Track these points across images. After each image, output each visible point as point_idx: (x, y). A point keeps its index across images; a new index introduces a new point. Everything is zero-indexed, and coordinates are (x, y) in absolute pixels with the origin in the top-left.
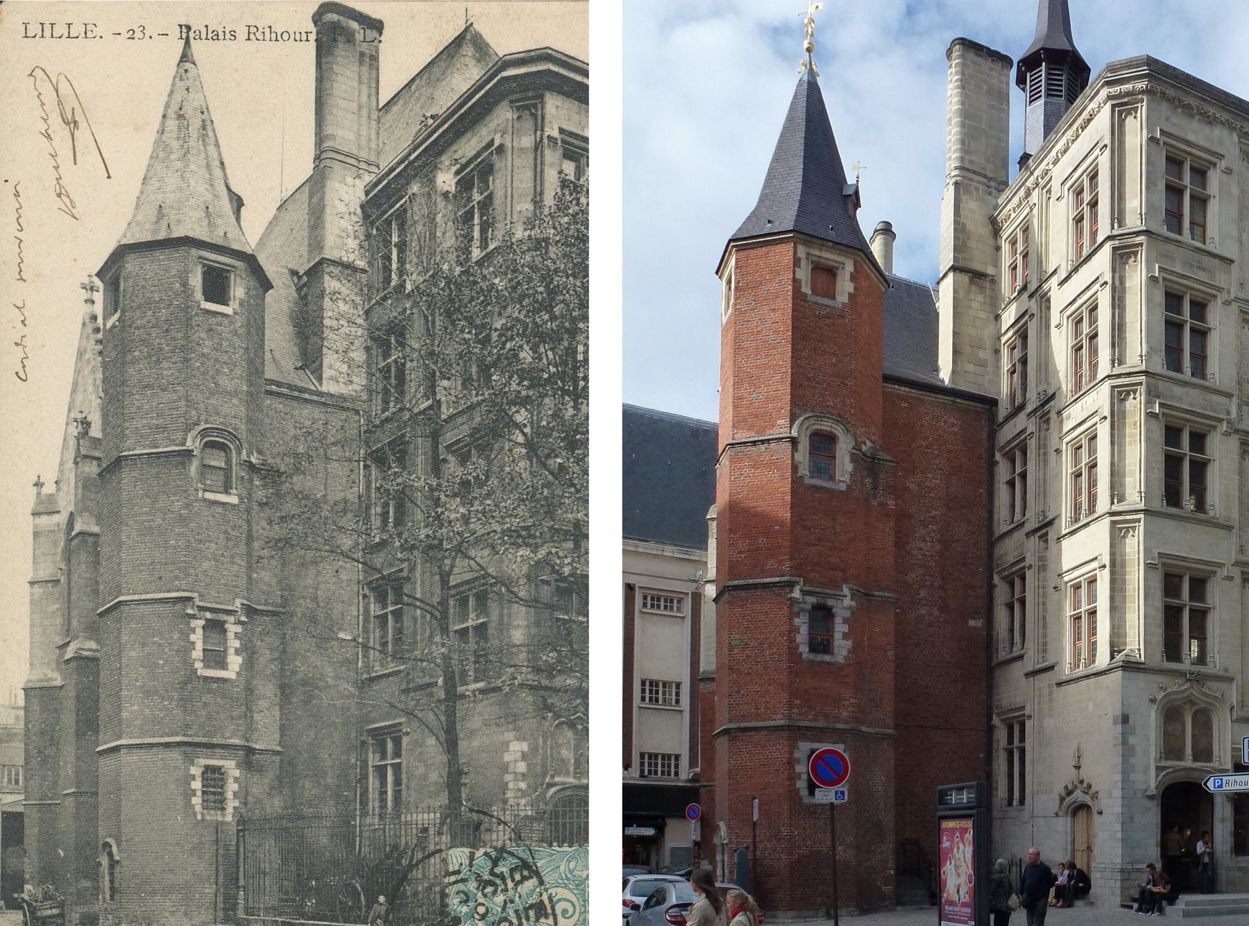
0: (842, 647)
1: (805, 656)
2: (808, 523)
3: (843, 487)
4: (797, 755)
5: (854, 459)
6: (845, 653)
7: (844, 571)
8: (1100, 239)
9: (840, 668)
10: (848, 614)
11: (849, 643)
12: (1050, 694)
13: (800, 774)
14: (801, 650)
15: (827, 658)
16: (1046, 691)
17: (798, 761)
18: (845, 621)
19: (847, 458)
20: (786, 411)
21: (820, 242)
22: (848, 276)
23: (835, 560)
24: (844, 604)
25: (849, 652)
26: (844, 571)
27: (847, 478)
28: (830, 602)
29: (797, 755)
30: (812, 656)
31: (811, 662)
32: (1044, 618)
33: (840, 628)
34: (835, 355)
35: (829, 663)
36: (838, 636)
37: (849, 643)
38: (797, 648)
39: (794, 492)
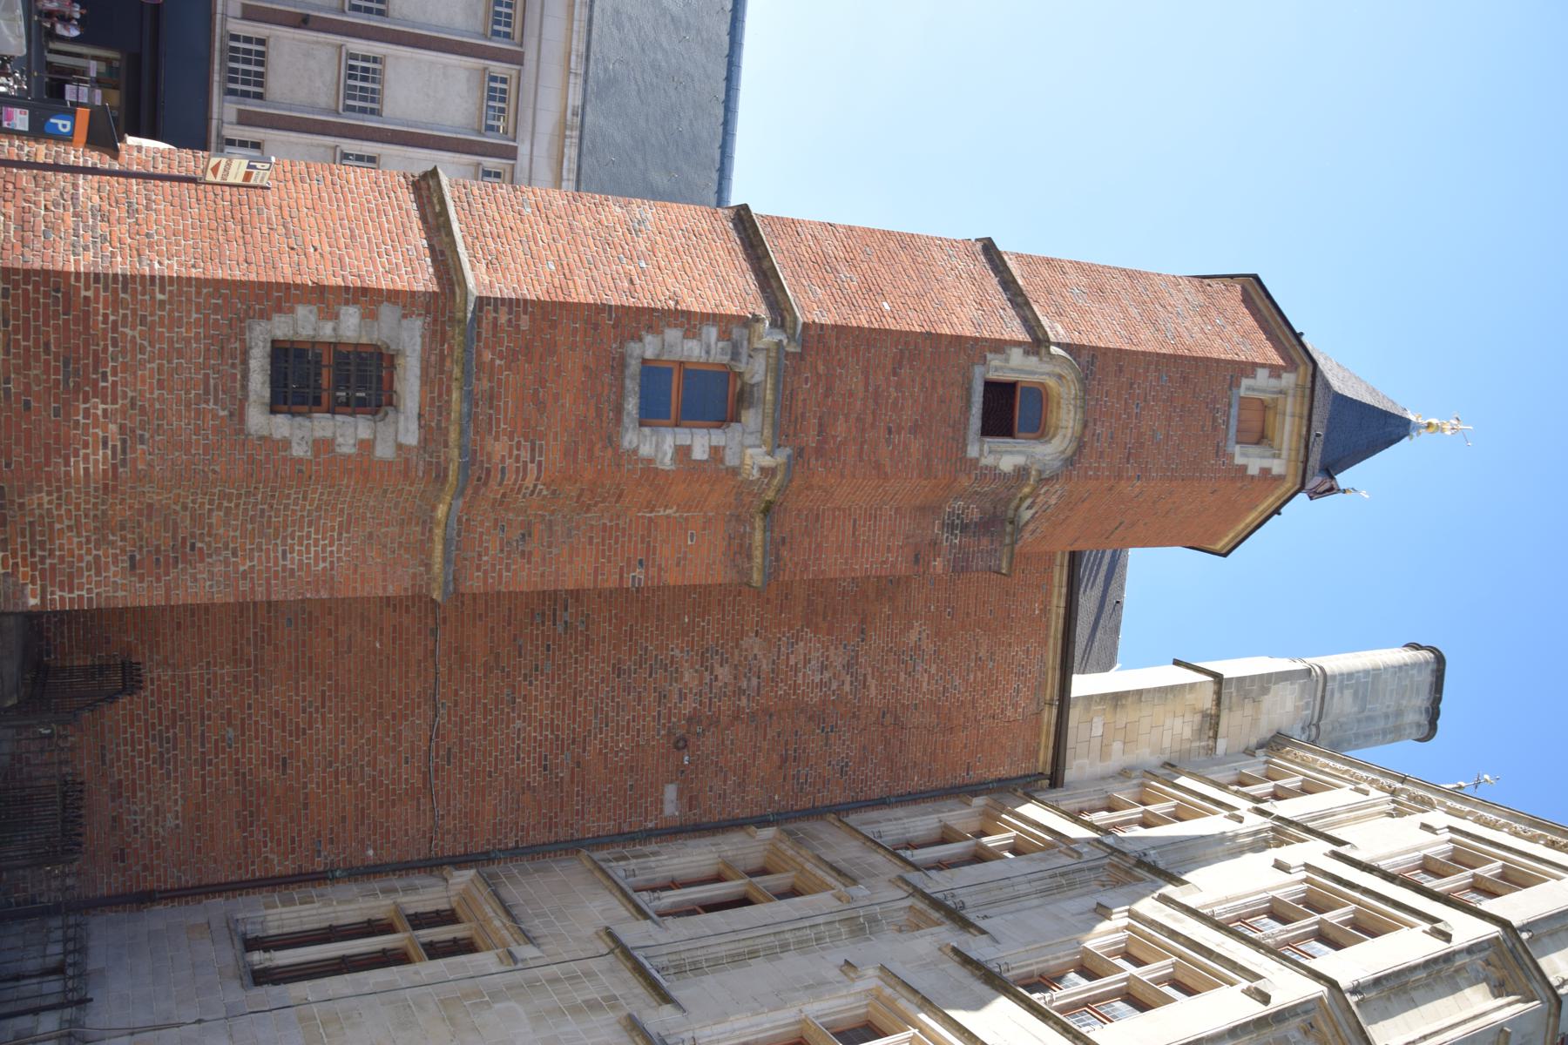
0: (658, 446)
1: (634, 349)
2: (905, 371)
3: (973, 451)
4: (388, 312)
5: (1021, 473)
6: (646, 450)
7: (819, 451)
8: (1488, 905)
9: (611, 441)
10: (731, 460)
11: (666, 461)
12: (593, 1006)
13: (336, 316)
14: (648, 338)
15: (632, 405)
16: (592, 992)
17: (370, 315)
18: (716, 452)
19: (1020, 460)
20: (1076, 338)
21: (1306, 413)
22: (1266, 463)
23: (840, 429)
24: (749, 448)
25: (650, 461)
26: (819, 451)
27: (988, 460)
28: (751, 418)
29: (388, 312)
30: (634, 366)
31: (621, 363)
32: (753, 954)
33: (701, 442)
34: (1168, 436)
35: (619, 410)
36: (683, 436)
37: (666, 461)
38: (651, 329)
39: (958, 340)
